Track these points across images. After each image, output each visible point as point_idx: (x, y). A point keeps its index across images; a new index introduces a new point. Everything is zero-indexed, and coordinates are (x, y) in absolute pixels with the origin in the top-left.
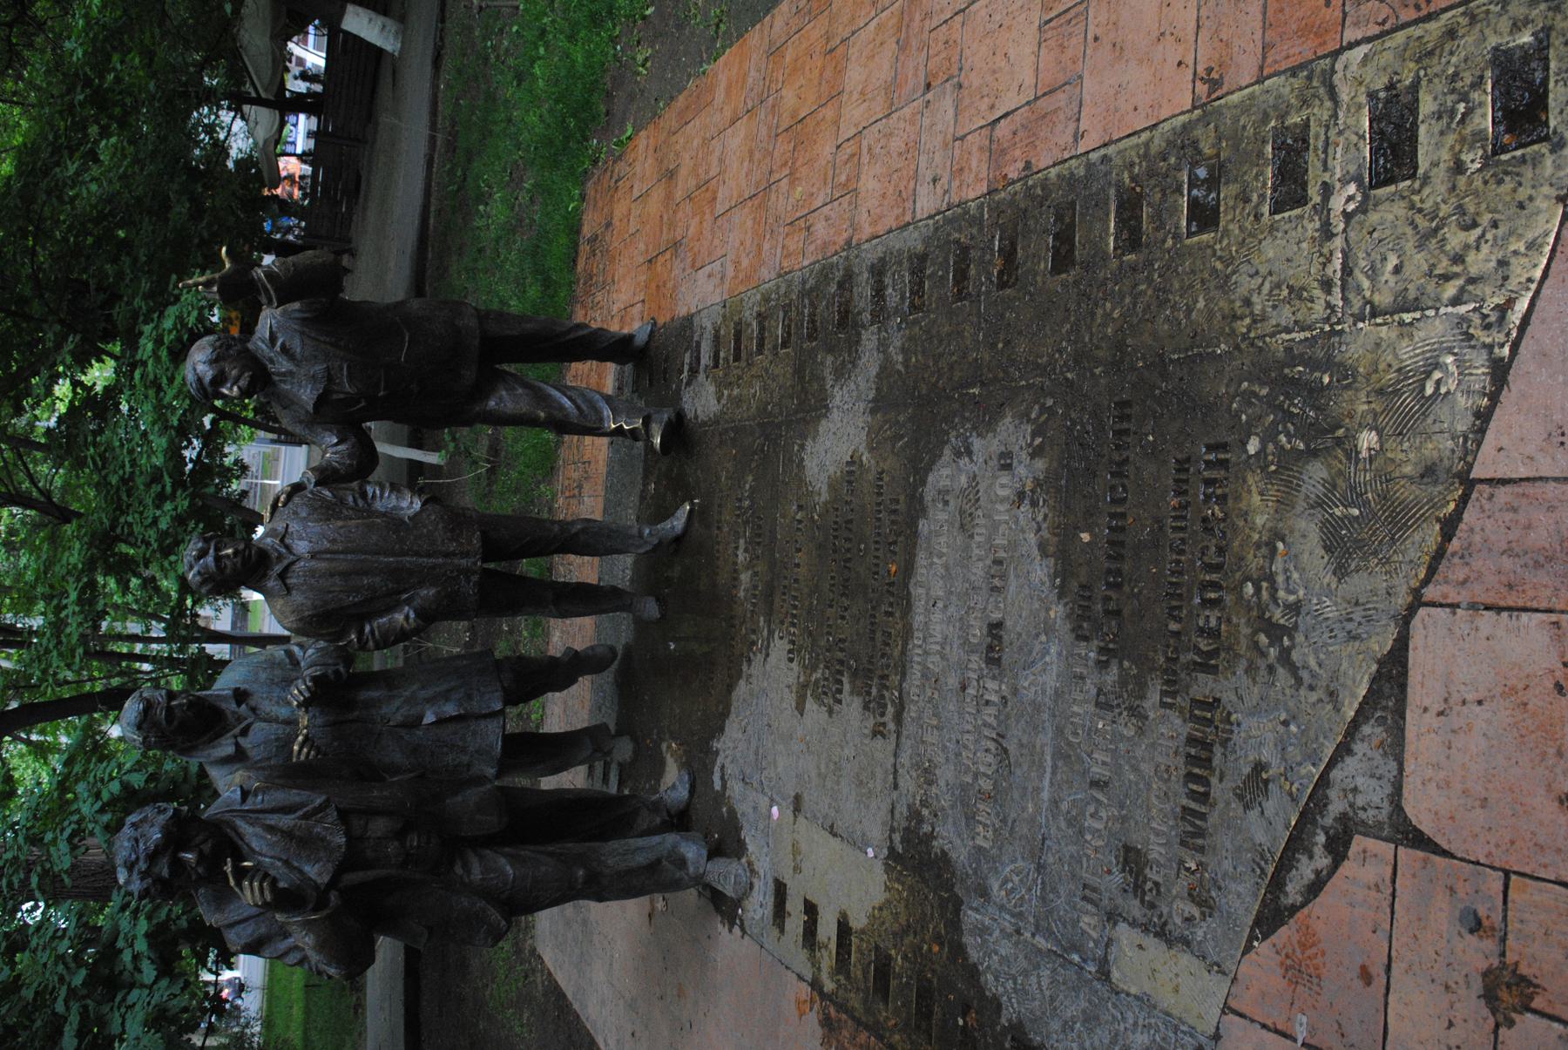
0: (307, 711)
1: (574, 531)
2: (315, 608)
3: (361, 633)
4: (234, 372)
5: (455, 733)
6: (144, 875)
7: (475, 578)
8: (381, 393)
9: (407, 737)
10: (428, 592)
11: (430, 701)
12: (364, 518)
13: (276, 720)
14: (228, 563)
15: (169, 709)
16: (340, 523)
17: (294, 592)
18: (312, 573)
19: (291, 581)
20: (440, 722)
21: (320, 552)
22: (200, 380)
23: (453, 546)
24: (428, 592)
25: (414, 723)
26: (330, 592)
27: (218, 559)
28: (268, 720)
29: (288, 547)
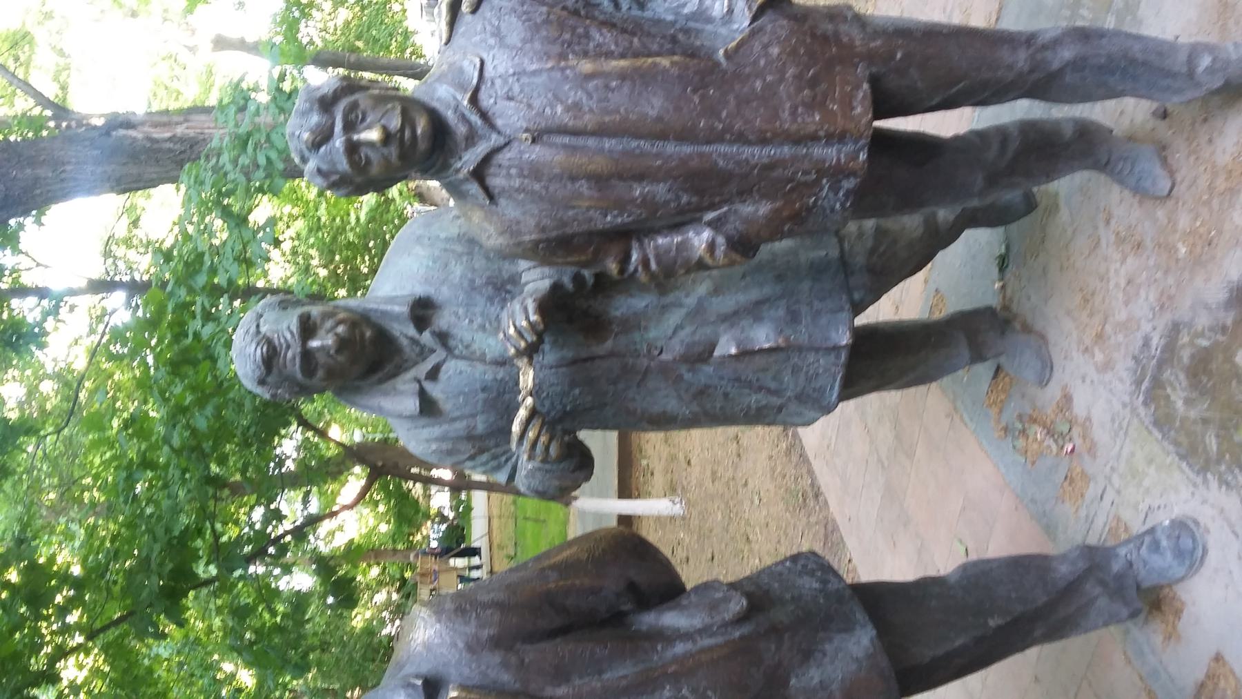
0: (530, 363)
1: (1056, 65)
2: (543, 230)
3: (625, 260)
5: (765, 370)
7: (849, 184)
9: (688, 376)
11: (731, 318)
12: (636, 55)
13: (482, 359)
14: (373, 156)
15: (307, 355)
16: (586, 66)
17: (503, 202)
18: (534, 171)
19: (496, 181)
20: (746, 354)
21: (550, 131)
24: (757, 210)
25: (701, 355)
26: (574, 207)
27: (352, 148)
28: (469, 358)
29: (484, 115)
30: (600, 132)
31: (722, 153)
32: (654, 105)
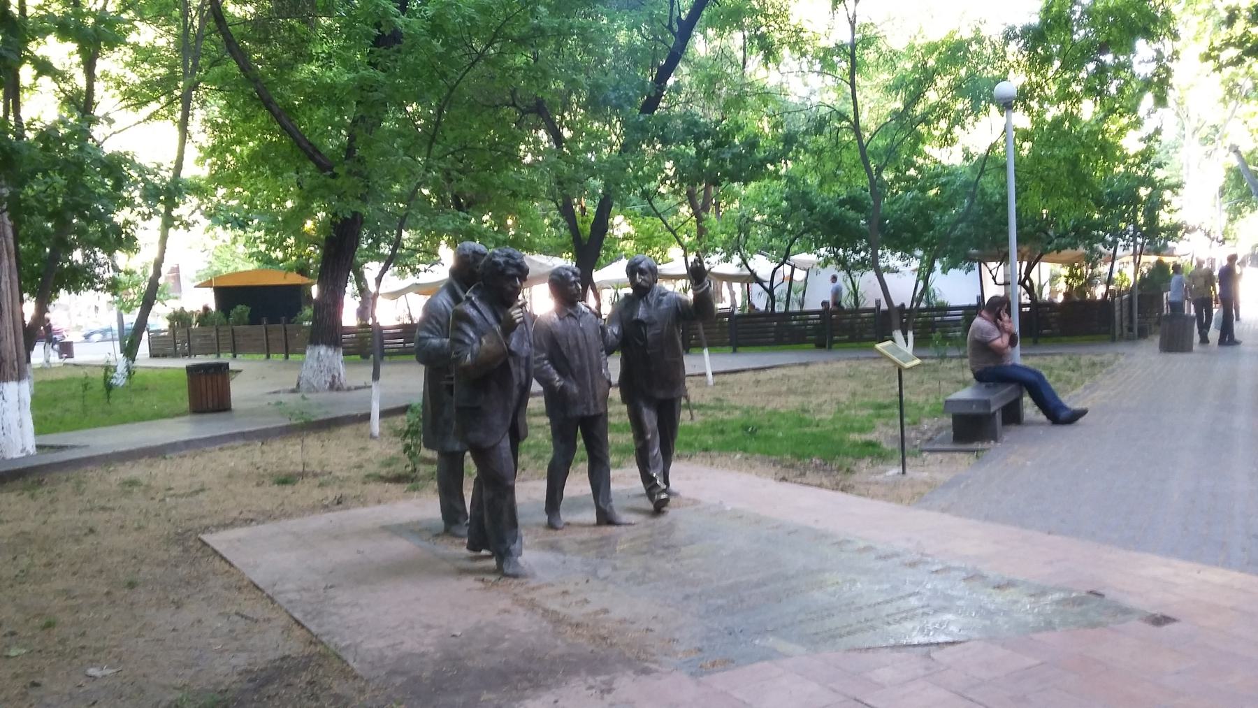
3: (545, 359)
4: (646, 278)
6: (506, 263)
7: (586, 413)
8: (648, 352)
10: (575, 389)
22: (640, 263)
23: (598, 398)
27: (575, 282)
30: (586, 343)
31: (589, 377)
32: (595, 357)
